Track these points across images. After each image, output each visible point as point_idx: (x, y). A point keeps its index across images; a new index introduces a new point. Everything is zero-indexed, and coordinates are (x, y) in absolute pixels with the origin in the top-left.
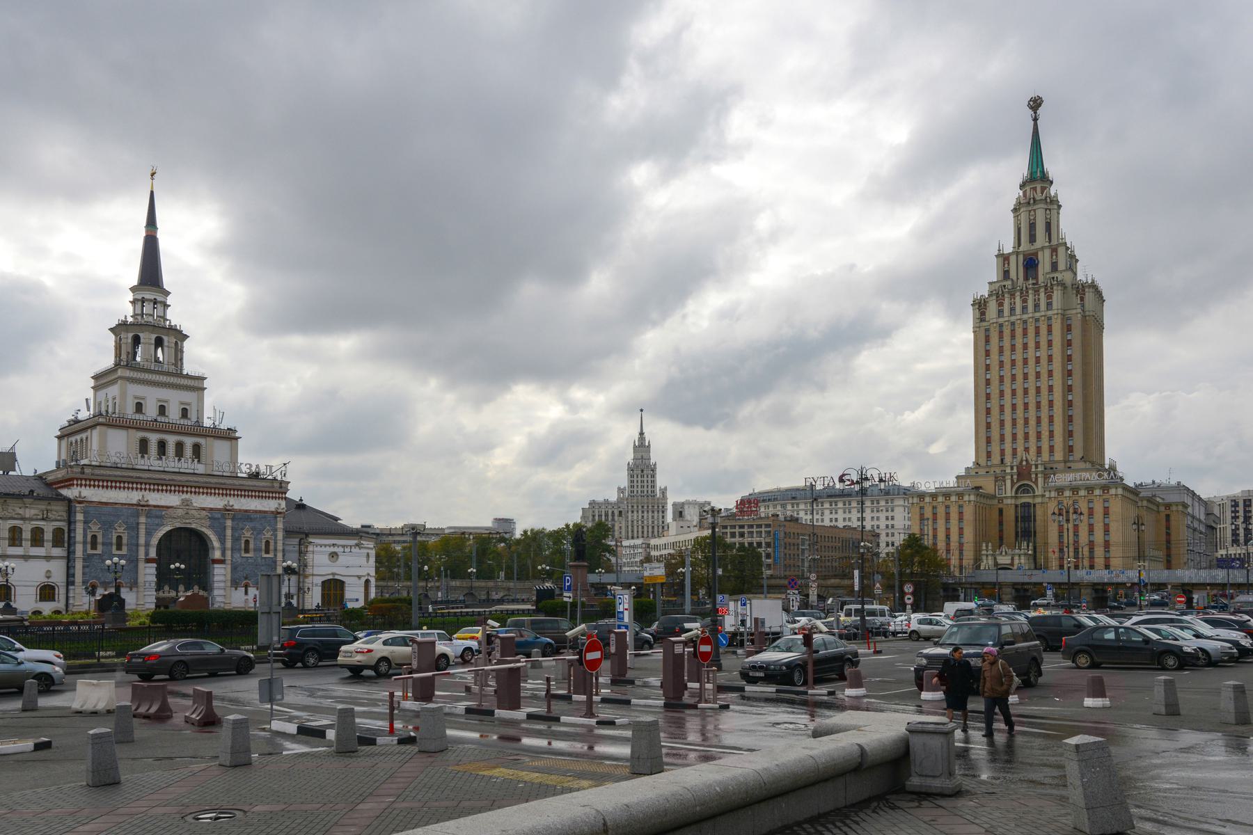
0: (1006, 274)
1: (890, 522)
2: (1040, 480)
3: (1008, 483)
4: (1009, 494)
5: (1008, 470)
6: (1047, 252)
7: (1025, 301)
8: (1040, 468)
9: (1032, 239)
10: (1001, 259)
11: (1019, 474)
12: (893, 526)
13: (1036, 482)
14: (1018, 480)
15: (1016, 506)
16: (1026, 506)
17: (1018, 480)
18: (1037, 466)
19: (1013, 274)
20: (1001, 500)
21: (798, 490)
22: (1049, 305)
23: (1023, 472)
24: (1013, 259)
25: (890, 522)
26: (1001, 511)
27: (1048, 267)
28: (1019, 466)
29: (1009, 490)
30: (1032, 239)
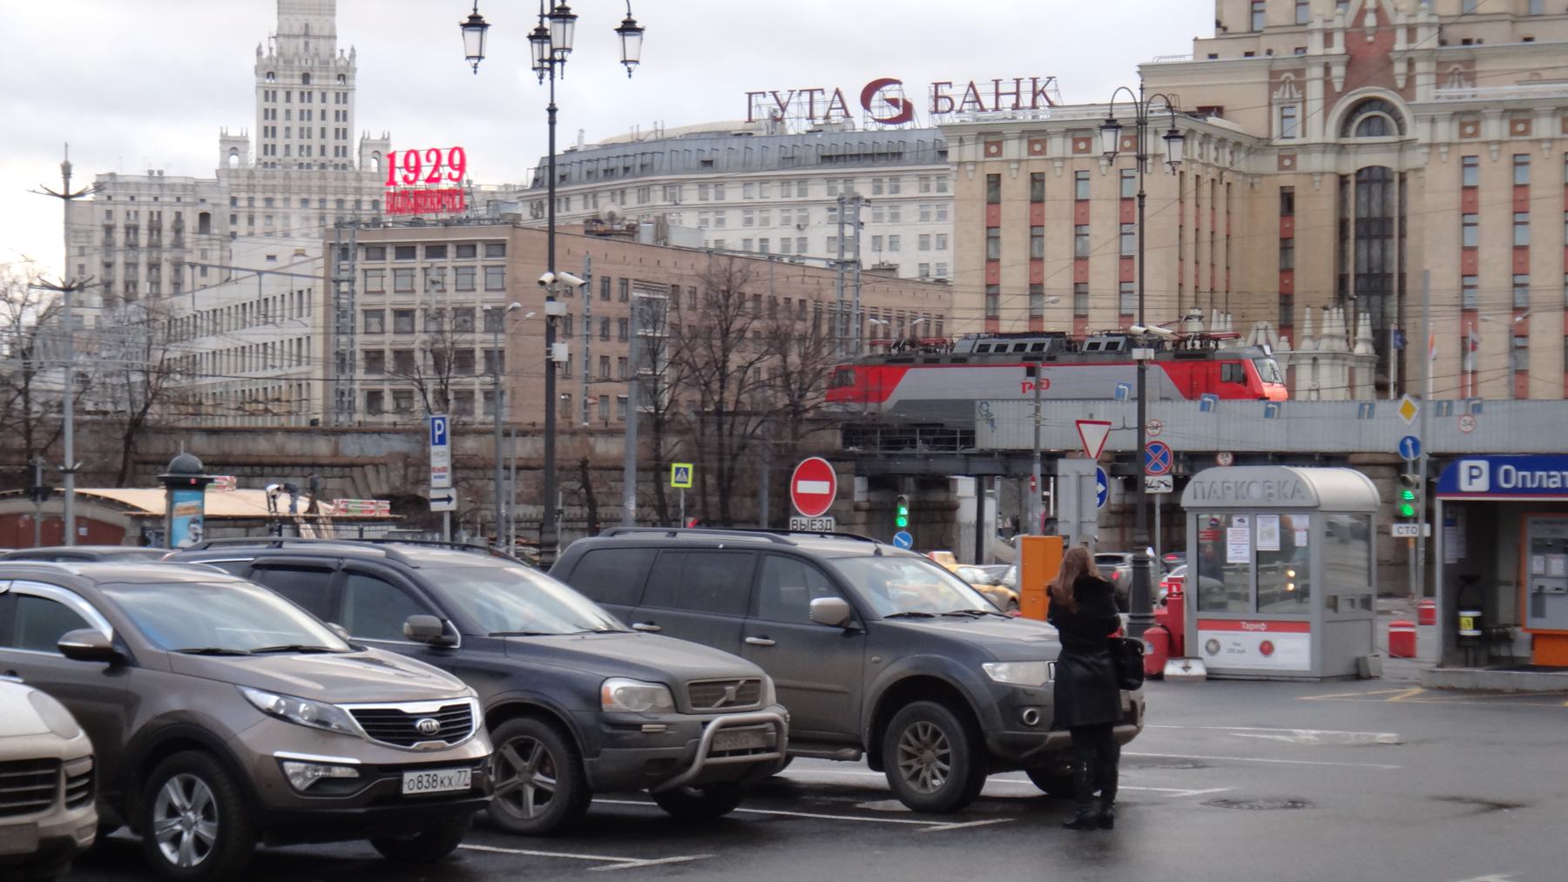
3: (1315, 90)
4: (1315, 136)
5: (1315, 47)
8: (1426, 40)
11: (1351, 63)
13: (1408, 91)
14: (1348, 86)
15: (1343, 180)
16: (1372, 178)
17: (1348, 86)
20: (1287, 157)
21: (722, 135)
23: (1366, 55)
26: (1288, 200)
28: (1354, 34)
29: (1319, 126)
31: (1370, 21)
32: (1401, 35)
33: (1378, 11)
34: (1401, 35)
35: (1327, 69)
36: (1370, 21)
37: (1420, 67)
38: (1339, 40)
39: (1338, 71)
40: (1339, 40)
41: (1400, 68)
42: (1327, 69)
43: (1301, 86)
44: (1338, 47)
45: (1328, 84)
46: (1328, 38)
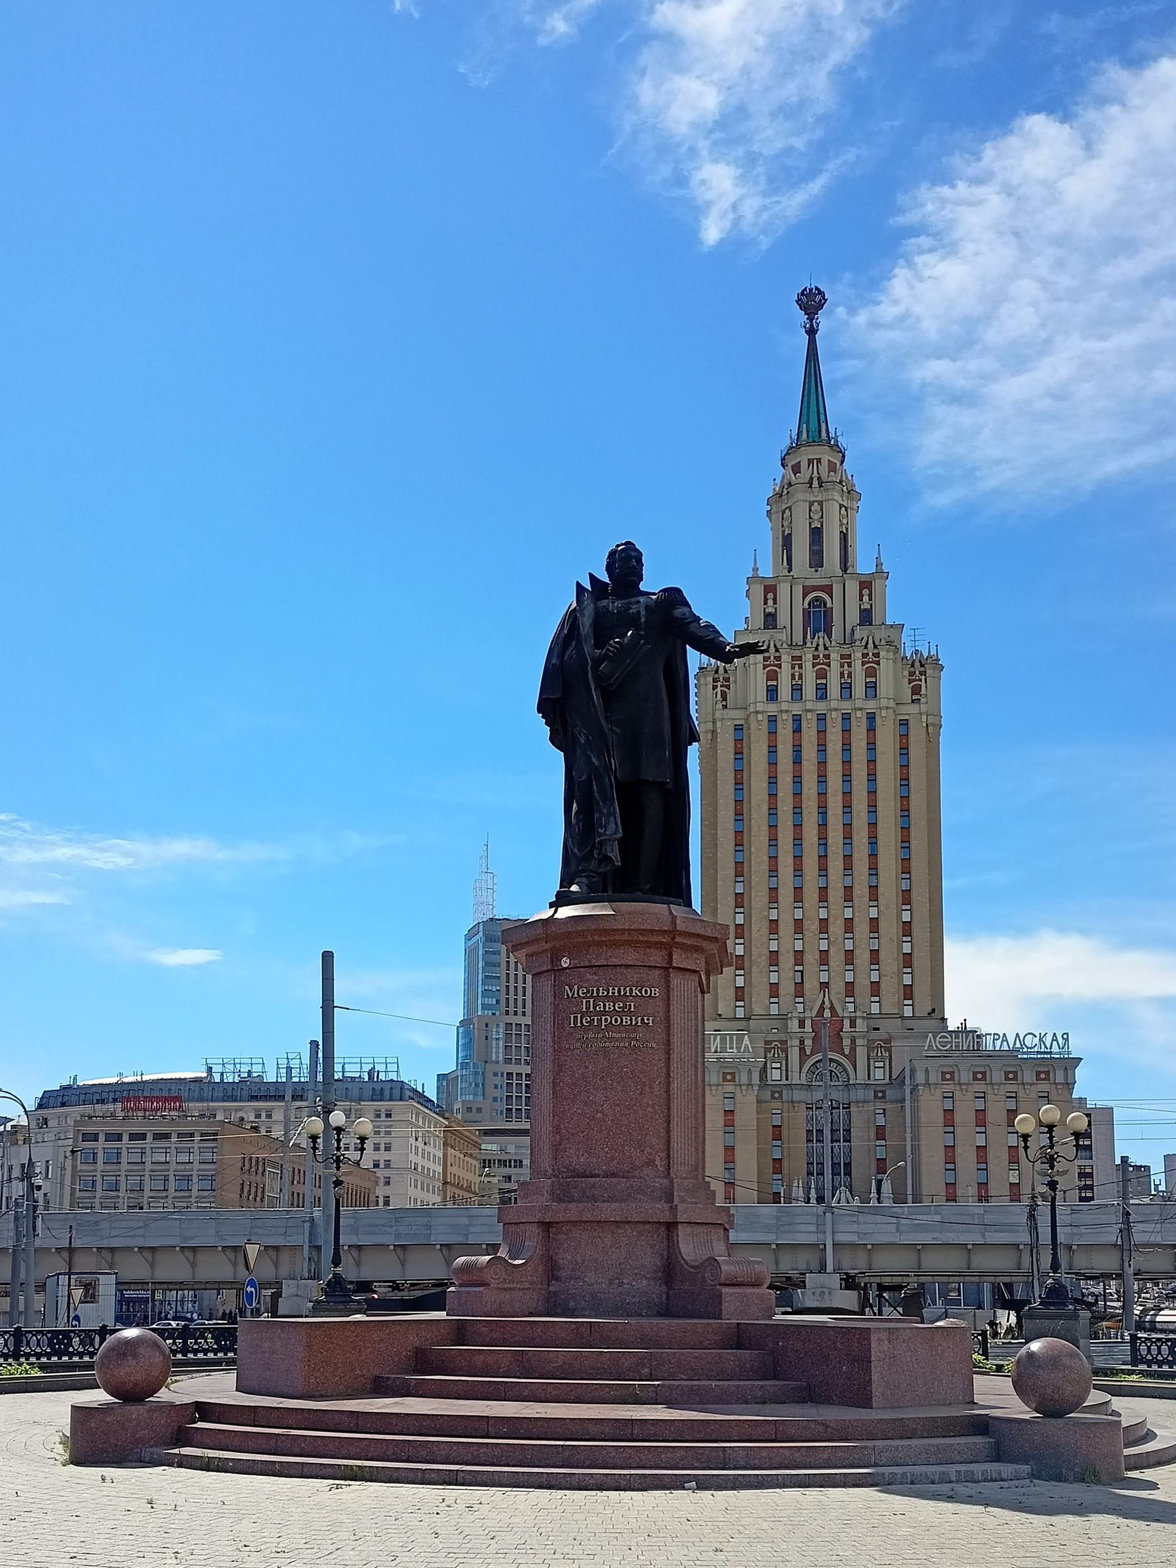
0: (770, 620)
1: (382, 1156)
2: (861, 1053)
3: (794, 1054)
5: (794, 1025)
6: (853, 587)
7: (822, 674)
9: (817, 560)
10: (759, 591)
12: (388, 1164)
14: (812, 1054)
18: (853, 1024)
19: (783, 619)
22: (872, 689)
23: (829, 1031)
24: (783, 590)
25: (382, 1156)
27: (853, 617)
30: (817, 560)
31: (827, 1013)
32: (847, 1023)
33: (832, 1008)
34: (847, 1023)
35: (802, 1042)
36: (827, 1013)
37: (859, 1042)
38: (808, 1023)
39: (808, 1042)
40: (808, 1023)
41: (846, 1042)
42: (802, 1042)
43: (785, 1051)
44: (808, 1027)
45: (802, 1049)
46: (802, 1024)
